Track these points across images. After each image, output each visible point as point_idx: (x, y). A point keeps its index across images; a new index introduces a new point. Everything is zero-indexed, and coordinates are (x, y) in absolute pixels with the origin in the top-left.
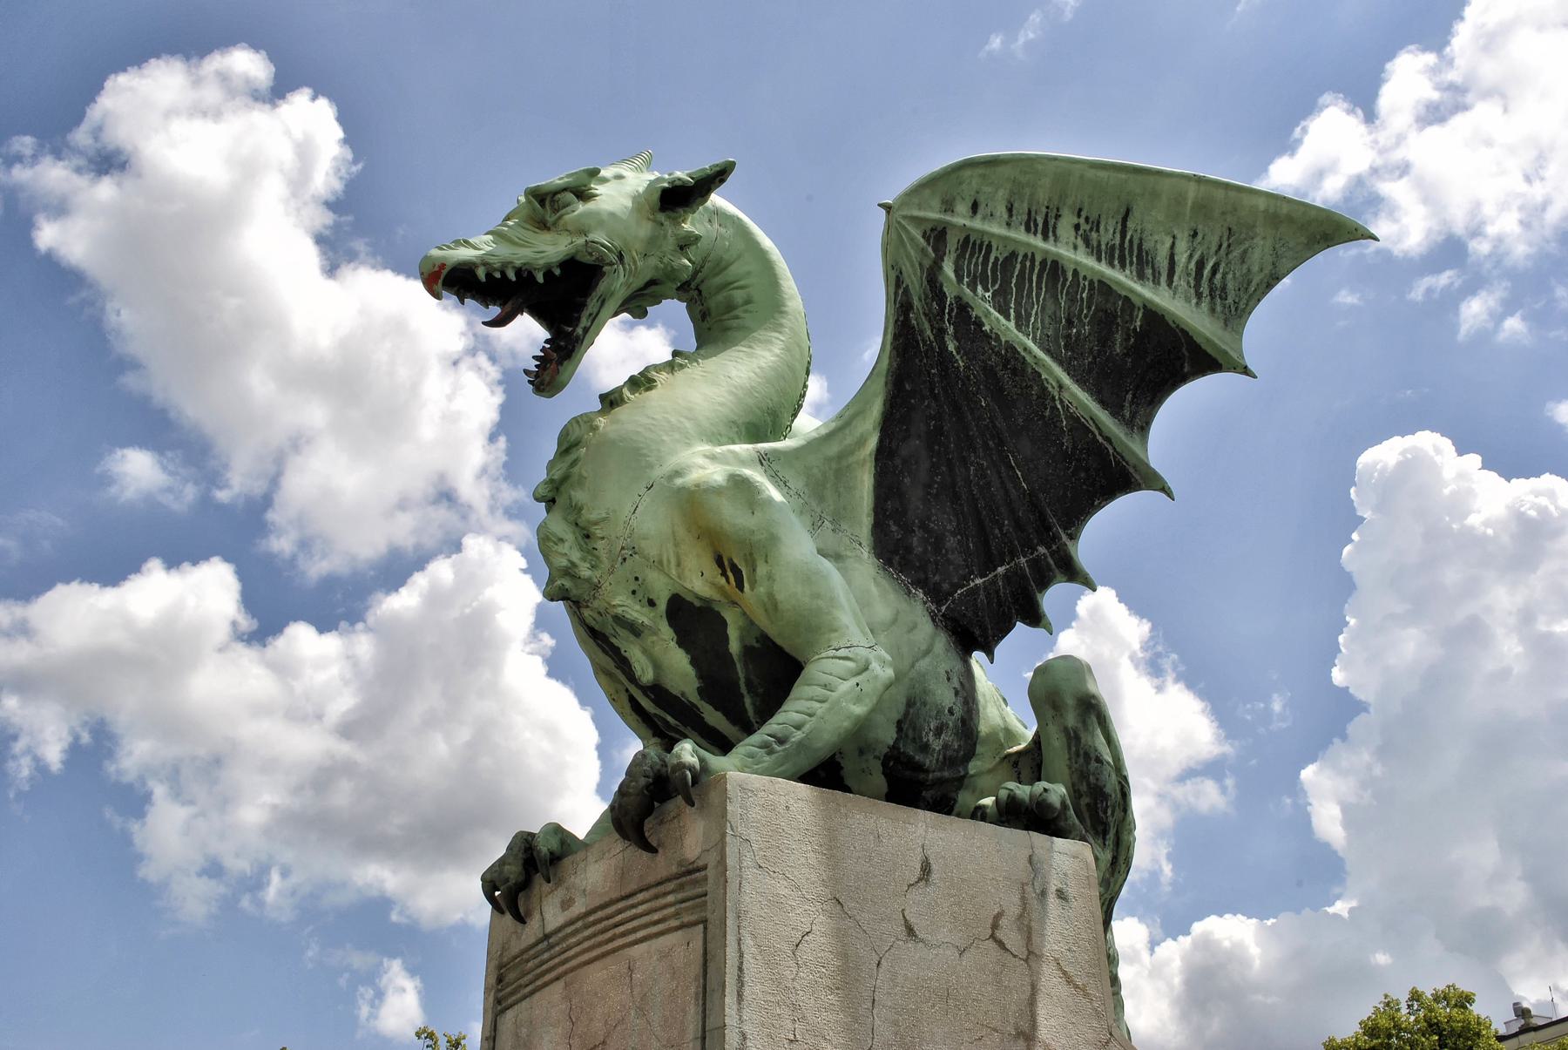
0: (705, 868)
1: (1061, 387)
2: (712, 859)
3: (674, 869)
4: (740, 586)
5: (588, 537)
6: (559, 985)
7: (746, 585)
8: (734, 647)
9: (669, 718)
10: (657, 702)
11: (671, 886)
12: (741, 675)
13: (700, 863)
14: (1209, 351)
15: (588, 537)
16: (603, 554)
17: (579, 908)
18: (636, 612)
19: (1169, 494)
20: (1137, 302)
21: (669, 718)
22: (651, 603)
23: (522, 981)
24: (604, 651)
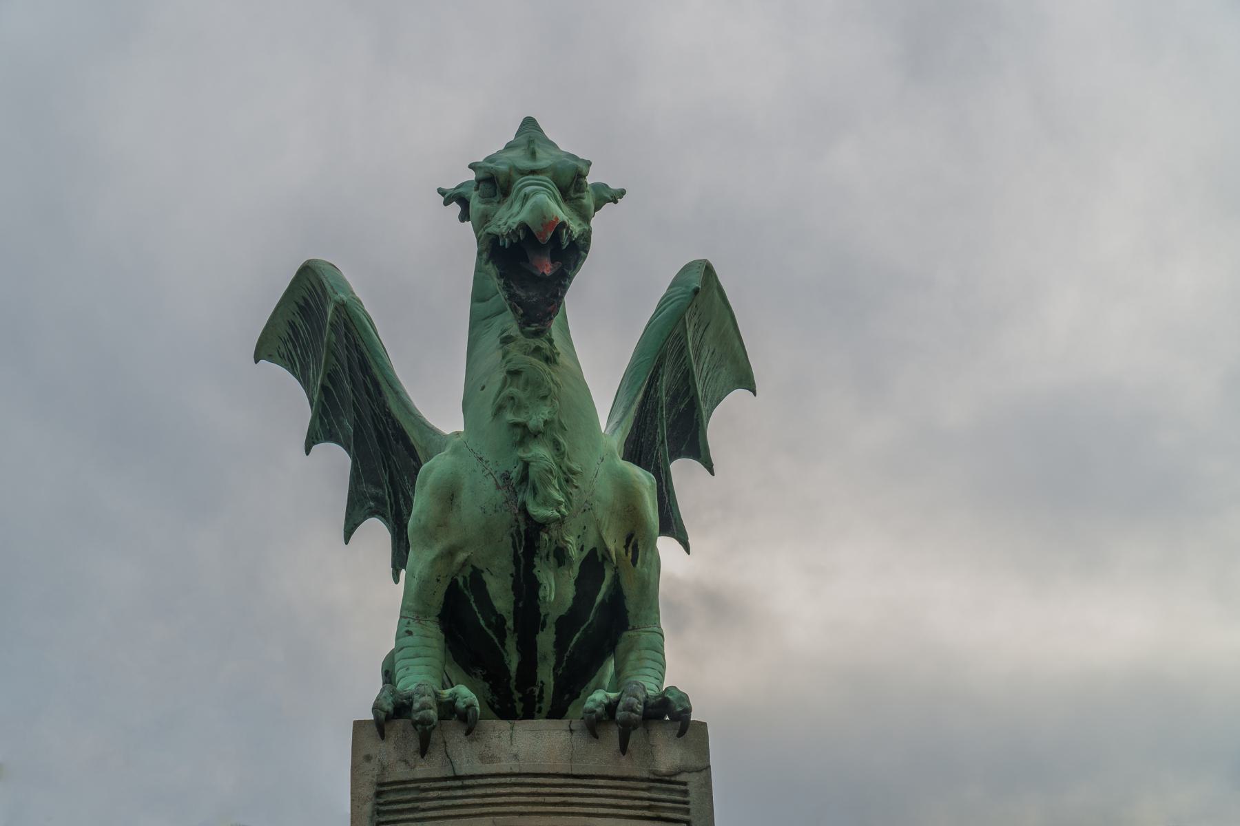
0: (685, 784)
1: (663, 442)
2: (693, 780)
3: (645, 774)
4: (634, 561)
5: (567, 481)
6: (489, 819)
7: (639, 565)
8: (599, 598)
9: (510, 624)
10: (517, 612)
11: (644, 785)
12: (591, 618)
13: (679, 778)
14: (701, 447)
15: (567, 481)
16: (574, 499)
17: (505, 766)
18: (573, 551)
19: (687, 550)
20: (691, 393)
21: (510, 624)
22: (582, 549)
23: (422, 805)
24: (516, 560)
